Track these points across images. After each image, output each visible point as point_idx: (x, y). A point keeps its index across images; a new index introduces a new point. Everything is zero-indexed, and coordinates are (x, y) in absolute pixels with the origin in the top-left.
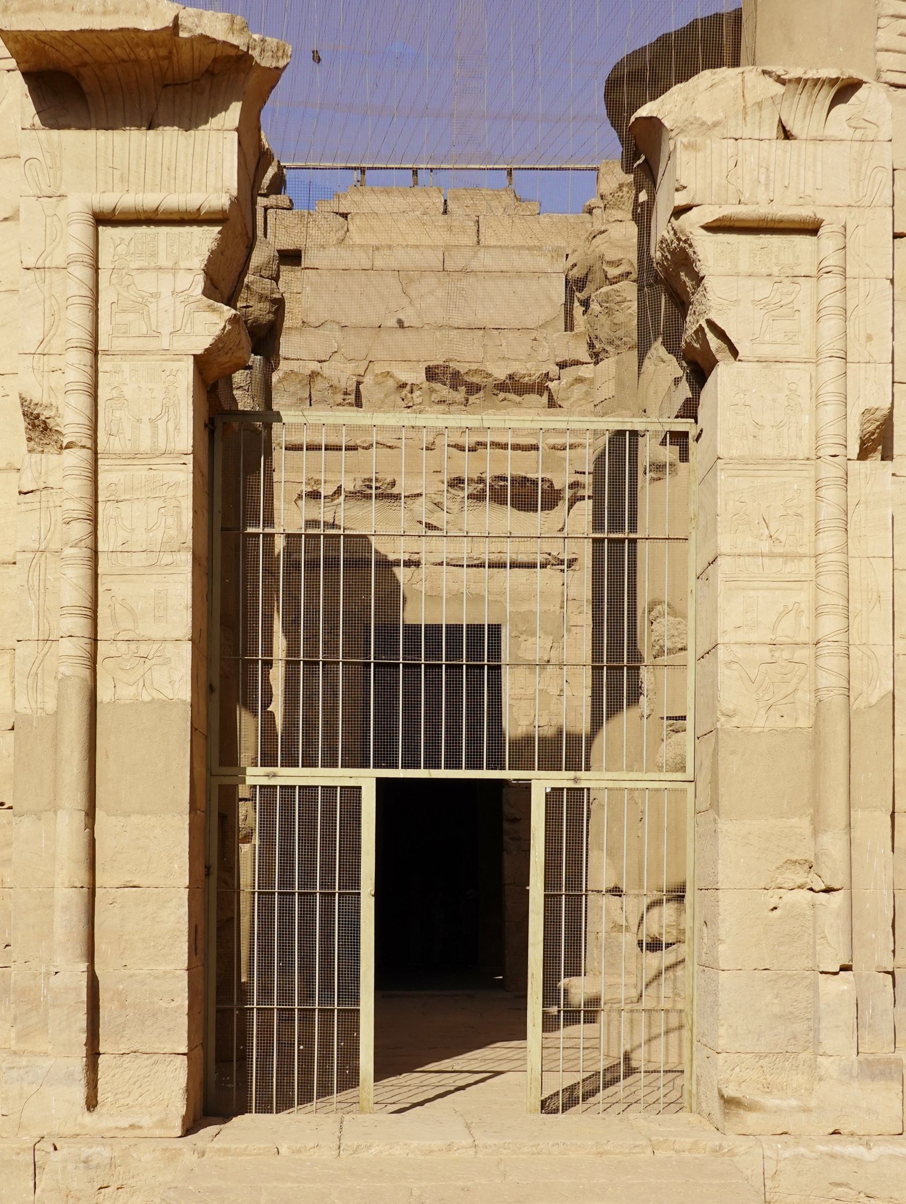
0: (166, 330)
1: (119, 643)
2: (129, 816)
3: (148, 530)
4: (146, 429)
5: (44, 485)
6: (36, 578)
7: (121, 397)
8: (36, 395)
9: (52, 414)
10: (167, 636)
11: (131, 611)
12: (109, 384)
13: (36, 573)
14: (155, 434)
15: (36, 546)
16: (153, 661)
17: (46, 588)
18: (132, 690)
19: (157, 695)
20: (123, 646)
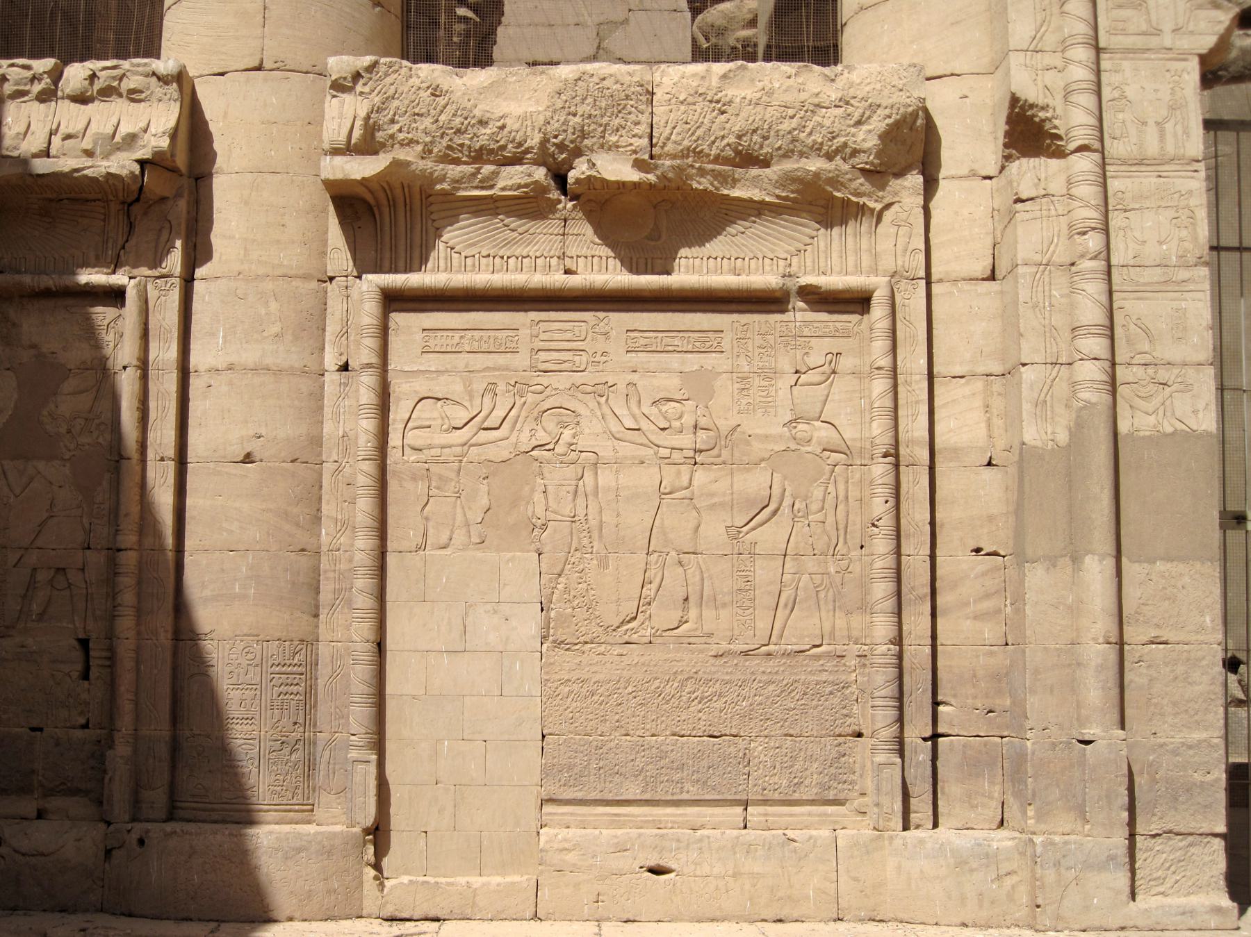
0: (1167, 27)
1: (1135, 369)
2: (1154, 563)
3: (1161, 243)
4: (1152, 130)
5: (1043, 192)
6: (1040, 295)
7: (1123, 96)
8: (1030, 93)
9: (1049, 115)
10: (1188, 359)
11: (1146, 331)
12: (1110, 84)
13: (1040, 289)
14: (1162, 138)
15: (1038, 258)
16: (1174, 388)
17: (1051, 305)
18: (1152, 420)
19: (1180, 426)
20: (1140, 371)
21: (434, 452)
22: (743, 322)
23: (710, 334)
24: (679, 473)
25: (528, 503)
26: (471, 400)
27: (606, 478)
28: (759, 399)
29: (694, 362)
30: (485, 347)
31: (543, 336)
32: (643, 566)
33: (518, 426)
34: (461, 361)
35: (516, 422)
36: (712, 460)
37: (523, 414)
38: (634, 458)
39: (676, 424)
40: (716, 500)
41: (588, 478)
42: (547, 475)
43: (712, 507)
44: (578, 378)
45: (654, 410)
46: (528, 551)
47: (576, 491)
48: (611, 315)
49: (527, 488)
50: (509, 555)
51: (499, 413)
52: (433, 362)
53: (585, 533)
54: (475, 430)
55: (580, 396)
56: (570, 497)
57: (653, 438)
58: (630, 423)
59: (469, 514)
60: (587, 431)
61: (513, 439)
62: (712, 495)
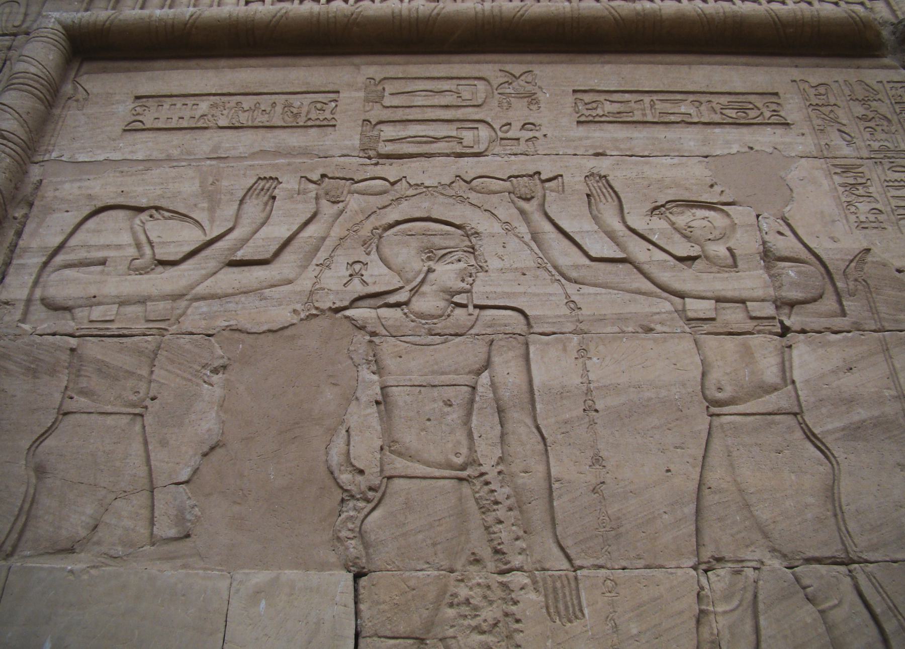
21: (97, 313)
22: (814, 81)
23: (751, 98)
24: (747, 353)
25: (332, 432)
26: (212, 210)
27: (552, 367)
28: (894, 203)
29: (729, 141)
30: (262, 119)
31: (387, 101)
32: (689, 602)
33: (321, 256)
34: (204, 143)
35: (317, 249)
36: (824, 322)
37: (337, 232)
38: (621, 319)
39: (719, 250)
40: (861, 414)
41: (507, 370)
42: (390, 363)
43: (854, 432)
44: (469, 167)
45: (657, 226)
46: (323, 566)
47: (472, 401)
48: (537, 70)
49: (329, 395)
50: (260, 577)
51: (278, 231)
52: (142, 146)
53: (501, 513)
54: (212, 265)
55: (474, 197)
56: (455, 415)
57: (665, 277)
58: (601, 247)
59: (158, 456)
60: (494, 264)
61: (305, 283)
62: (850, 402)
